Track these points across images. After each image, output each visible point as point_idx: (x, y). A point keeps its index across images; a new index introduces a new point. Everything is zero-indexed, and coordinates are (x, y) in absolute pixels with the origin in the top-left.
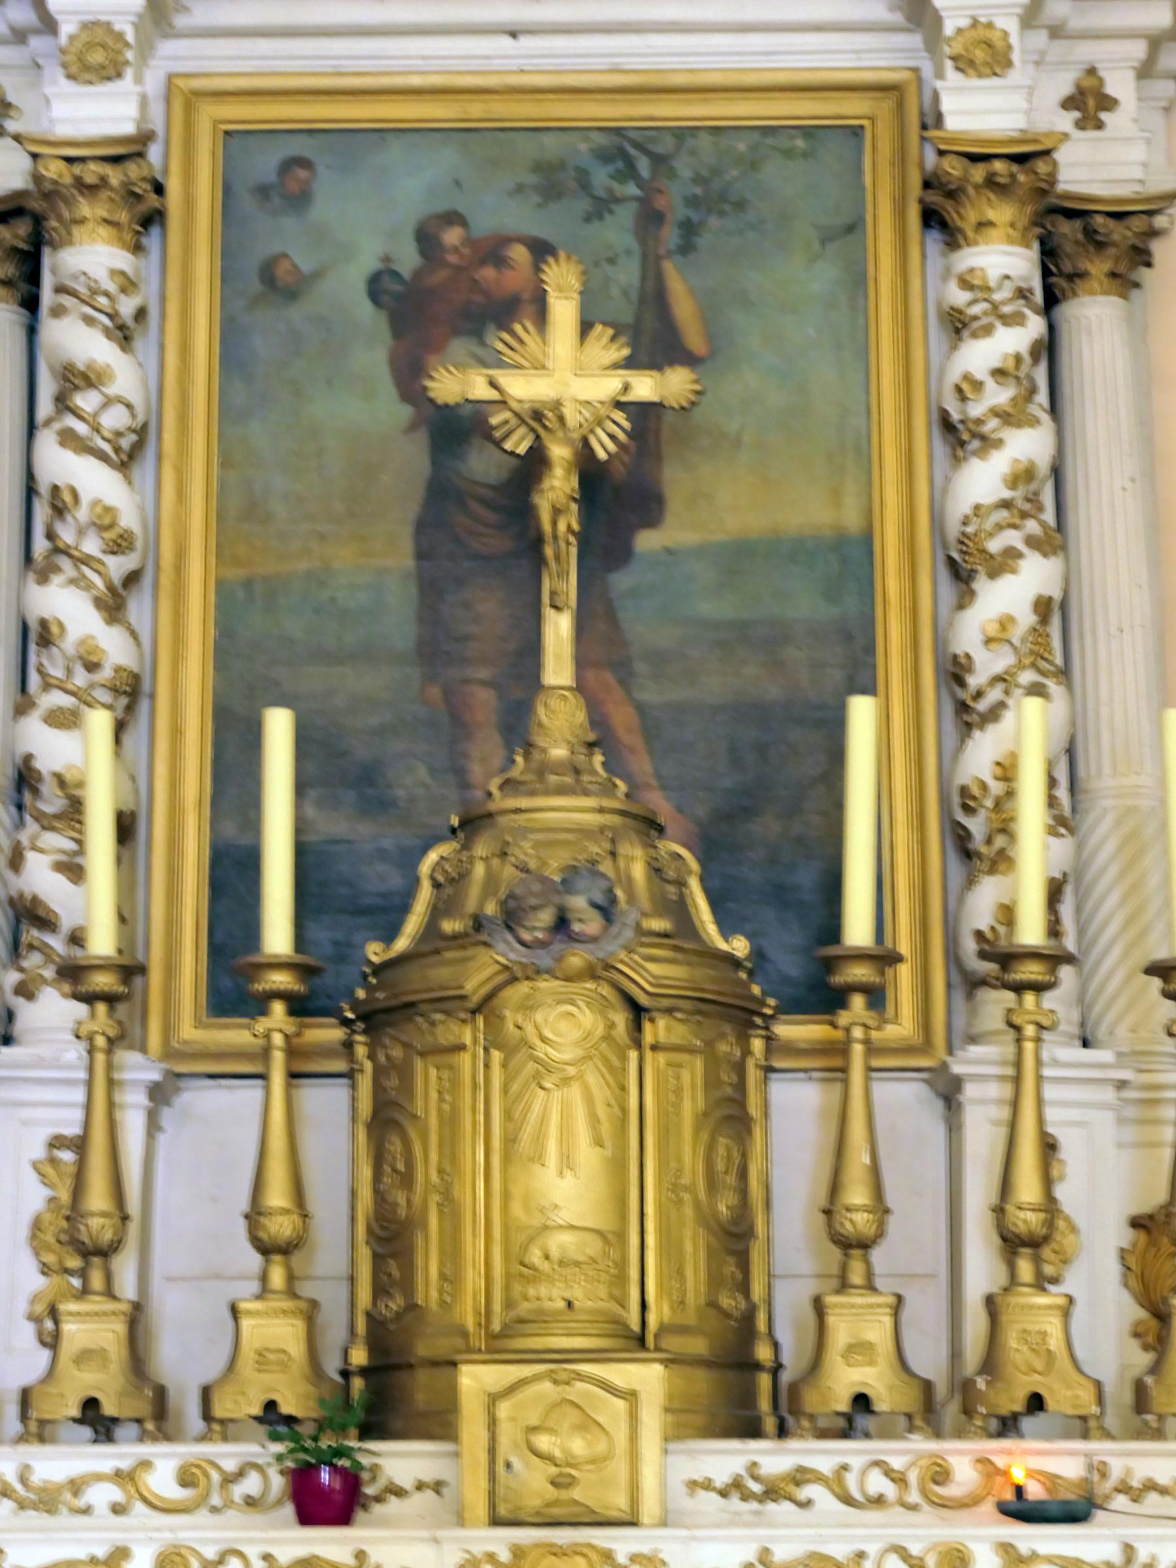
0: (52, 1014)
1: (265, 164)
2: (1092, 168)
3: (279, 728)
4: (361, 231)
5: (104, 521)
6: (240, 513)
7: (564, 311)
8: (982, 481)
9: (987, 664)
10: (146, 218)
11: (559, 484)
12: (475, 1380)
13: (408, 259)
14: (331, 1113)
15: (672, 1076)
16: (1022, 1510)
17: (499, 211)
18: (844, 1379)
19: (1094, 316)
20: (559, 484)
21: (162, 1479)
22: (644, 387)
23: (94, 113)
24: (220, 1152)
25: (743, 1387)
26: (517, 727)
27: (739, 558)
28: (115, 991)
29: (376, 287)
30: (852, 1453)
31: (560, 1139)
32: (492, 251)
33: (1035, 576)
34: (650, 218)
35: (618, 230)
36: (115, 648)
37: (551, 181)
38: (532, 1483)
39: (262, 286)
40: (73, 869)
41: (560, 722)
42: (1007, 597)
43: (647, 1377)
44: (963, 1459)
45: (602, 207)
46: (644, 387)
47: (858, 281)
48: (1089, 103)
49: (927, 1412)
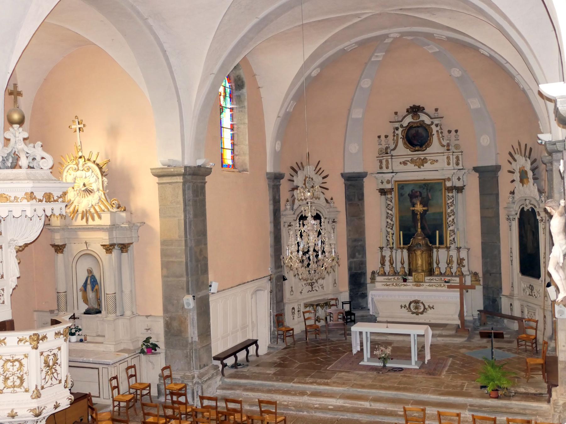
1: (401, 186)
2: (459, 184)
3: (401, 232)
4: (407, 191)
5: (391, 214)
6: (400, 211)
7: (419, 204)
9: (449, 223)
11: (419, 217)
12: (413, 274)
13: (411, 193)
15: (425, 255)
16: (446, 282)
17: (417, 189)
18: (436, 273)
19: (460, 194)
21: (396, 278)
22: (424, 208)
23: (389, 186)
24: (401, 255)
26: (417, 231)
27: (434, 213)
29: (409, 195)
30: (436, 278)
32: (416, 192)
33: (452, 217)
34: (427, 189)
35: (425, 190)
36: (392, 223)
37: (420, 187)
38: (417, 280)
39: (401, 195)
42: (451, 219)
43: (423, 274)
44: (443, 278)
45: (424, 189)
46: (424, 208)
47: (442, 194)
49: (441, 274)
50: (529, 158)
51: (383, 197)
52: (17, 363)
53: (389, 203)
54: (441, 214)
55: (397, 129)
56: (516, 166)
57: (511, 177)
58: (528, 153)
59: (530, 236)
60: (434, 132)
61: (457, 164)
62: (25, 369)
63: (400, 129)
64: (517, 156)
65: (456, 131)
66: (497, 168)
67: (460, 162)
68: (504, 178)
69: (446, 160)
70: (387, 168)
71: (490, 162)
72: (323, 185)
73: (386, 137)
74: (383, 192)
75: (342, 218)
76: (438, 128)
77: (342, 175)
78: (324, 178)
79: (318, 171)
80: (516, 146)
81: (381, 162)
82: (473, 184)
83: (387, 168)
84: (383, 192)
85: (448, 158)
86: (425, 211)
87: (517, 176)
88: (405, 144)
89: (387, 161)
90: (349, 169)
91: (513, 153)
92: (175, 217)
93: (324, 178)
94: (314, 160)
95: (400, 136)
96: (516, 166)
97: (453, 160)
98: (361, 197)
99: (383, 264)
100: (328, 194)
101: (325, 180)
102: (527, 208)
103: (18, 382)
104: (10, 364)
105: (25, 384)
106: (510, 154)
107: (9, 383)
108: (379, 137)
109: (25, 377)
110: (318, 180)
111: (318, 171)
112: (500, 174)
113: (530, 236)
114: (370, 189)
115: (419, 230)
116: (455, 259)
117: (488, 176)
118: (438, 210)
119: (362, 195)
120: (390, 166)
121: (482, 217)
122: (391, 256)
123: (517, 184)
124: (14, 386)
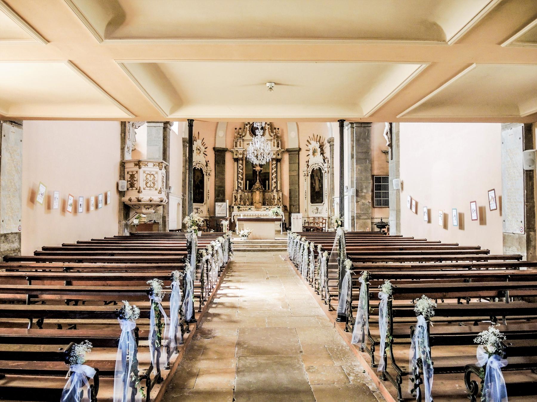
0: (240, 191)
2: (279, 157)
6: (246, 171)
8: (273, 171)
10: (242, 160)
11: (258, 173)
14: (250, 194)
15: (261, 194)
19: (279, 163)
20: (258, 173)
25: (264, 204)
28: (243, 191)
31: (258, 196)
40: (241, 185)
41: (258, 181)
48: (278, 155)
50: (319, 141)
51: (236, 163)
52: (152, 176)
53: (241, 165)
54: (269, 173)
55: (247, 125)
56: (311, 147)
57: (308, 153)
58: (319, 140)
59: (317, 182)
60: (267, 128)
61: (278, 147)
62: (156, 179)
63: (249, 125)
64: (312, 142)
65: (278, 129)
66: (300, 149)
67: (280, 145)
68: (303, 154)
69: (273, 144)
70: (240, 146)
71: (296, 146)
72: (205, 153)
73: (240, 129)
74: (236, 160)
75: (213, 174)
76: (269, 126)
77: (214, 148)
78: (206, 148)
79: (203, 144)
80: (312, 136)
81: (236, 143)
82: (286, 157)
83: (240, 146)
84: (236, 160)
85: (274, 143)
86: (261, 170)
87: (311, 153)
88: (250, 133)
89: (240, 142)
90: (218, 146)
91: (309, 140)
92: (156, 145)
93: (206, 148)
94: (201, 137)
95: (248, 129)
96: (311, 147)
97: (276, 144)
98: (224, 163)
99: (236, 199)
100: (208, 158)
101: (206, 150)
102: (316, 167)
103: (152, 185)
104: (149, 176)
105: (155, 186)
106: (308, 141)
107: (148, 185)
108: (236, 129)
109: (156, 183)
110: (203, 149)
111: (203, 144)
112: (300, 153)
113: (317, 182)
114: (228, 157)
115: (258, 181)
116: (276, 197)
117: (295, 153)
118: (267, 171)
119: (224, 161)
120: (242, 145)
121: (290, 176)
122: (241, 196)
123: (311, 156)
124: (150, 187)
